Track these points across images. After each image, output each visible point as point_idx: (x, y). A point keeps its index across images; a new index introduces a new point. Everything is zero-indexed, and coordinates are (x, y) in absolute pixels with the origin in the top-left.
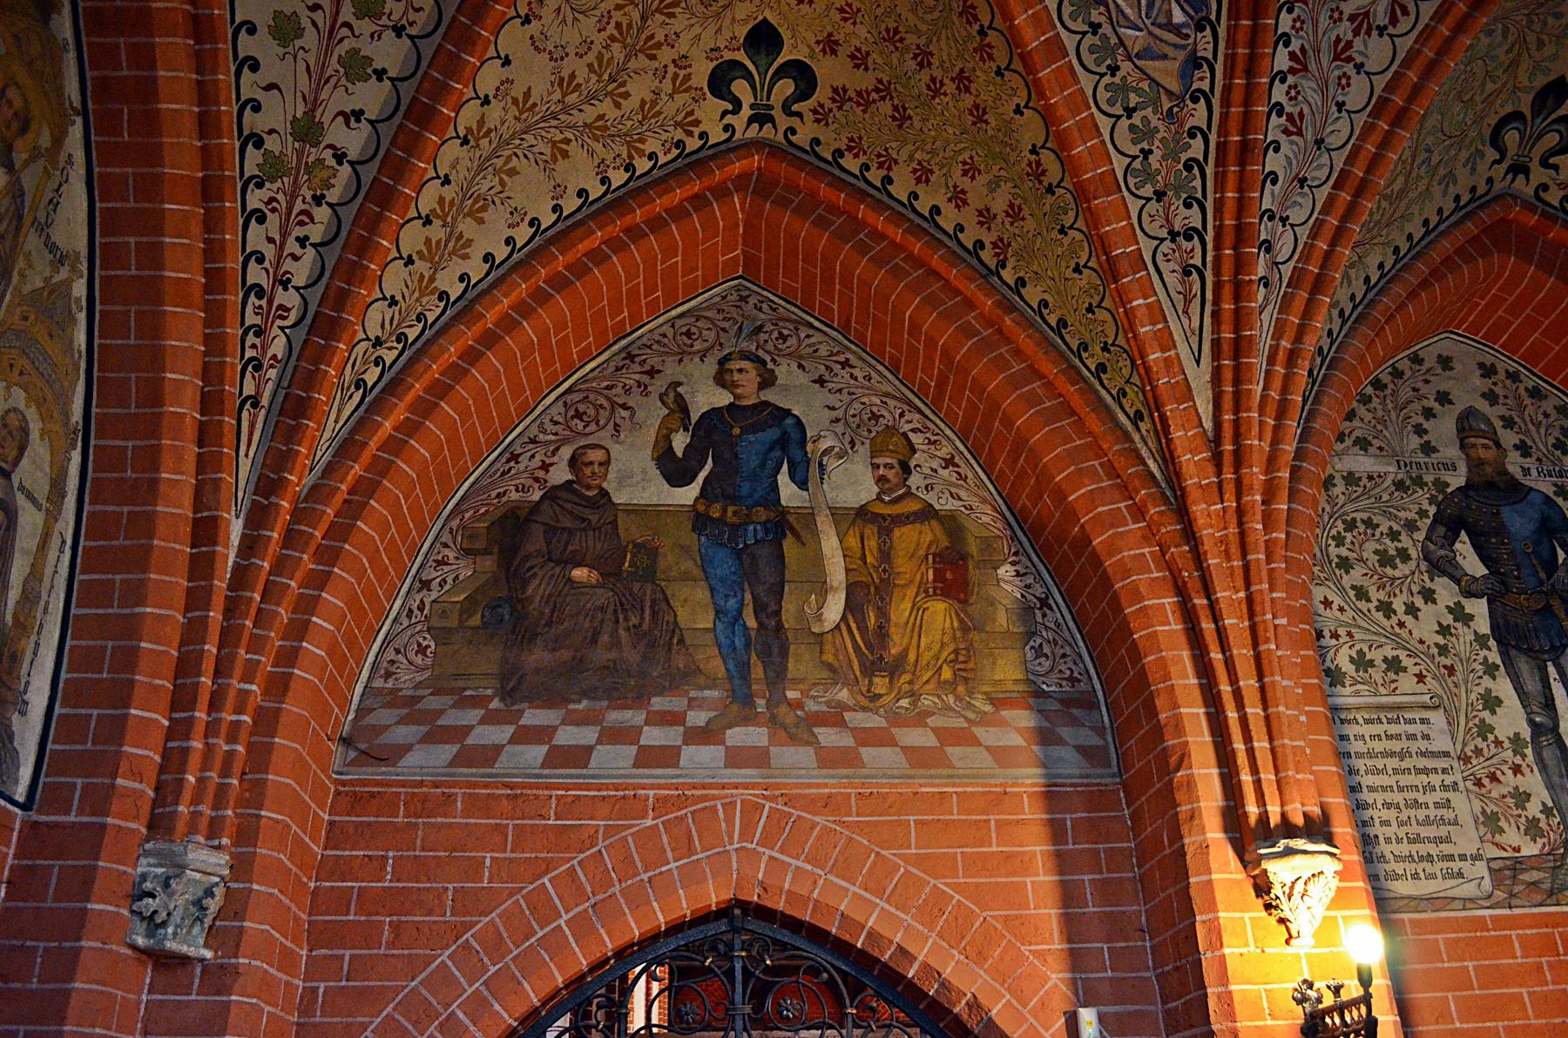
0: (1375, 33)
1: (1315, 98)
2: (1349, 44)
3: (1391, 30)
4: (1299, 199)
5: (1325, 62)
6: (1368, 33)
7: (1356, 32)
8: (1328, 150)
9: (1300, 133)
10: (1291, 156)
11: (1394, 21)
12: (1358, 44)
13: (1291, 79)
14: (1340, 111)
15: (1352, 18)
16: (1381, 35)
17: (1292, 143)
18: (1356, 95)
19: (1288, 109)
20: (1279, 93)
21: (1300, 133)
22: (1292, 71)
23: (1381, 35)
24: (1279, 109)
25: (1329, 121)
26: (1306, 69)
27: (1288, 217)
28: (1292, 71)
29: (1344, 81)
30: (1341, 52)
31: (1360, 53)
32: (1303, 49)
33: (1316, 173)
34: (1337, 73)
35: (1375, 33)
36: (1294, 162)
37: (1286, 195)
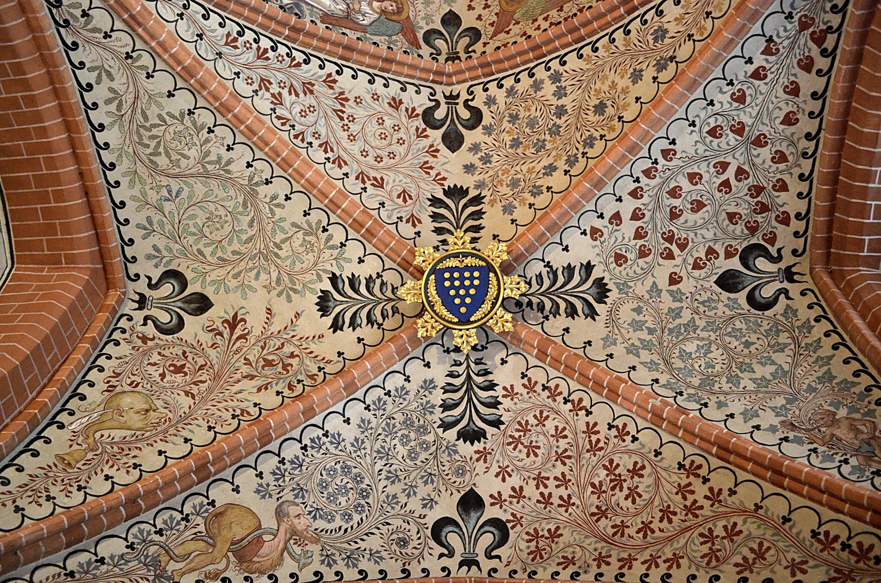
0: (272, 106)
1: (243, 59)
2: (267, 89)
3: (274, 116)
4: (191, 31)
5: (261, 71)
6: (272, 102)
7: (273, 95)
8: (215, 59)
9: (227, 44)
10: (215, 34)
11: (279, 118)
12: (268, 95)
13: (255, 46)
14: (235, 73)
15: (280, 94)
16: (271, 109)
17: (222, 36)
18: (242, 86)
19: (240, 39)
20: (249, 36)
21: (227, 44)
22: (259, 48)
23: (271, 109)
24: (241, 34)
25: (231, 66)
26: (259, 58)
27: (182, 19)
28: (259, 48)
29: (250, 81)
30: (265, 83)
31: (263, 95)
32: (268, 59)
33: (203, 47)
34: (254, 77)
35: (272, 106)
36: (212, 34)
37: (195, 22)
